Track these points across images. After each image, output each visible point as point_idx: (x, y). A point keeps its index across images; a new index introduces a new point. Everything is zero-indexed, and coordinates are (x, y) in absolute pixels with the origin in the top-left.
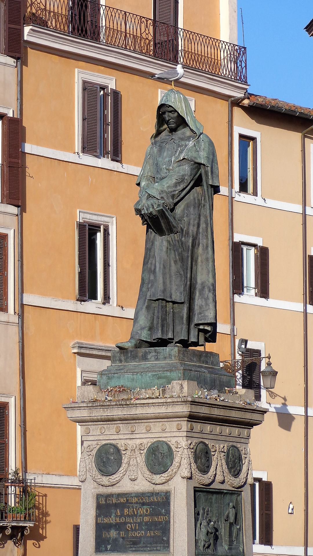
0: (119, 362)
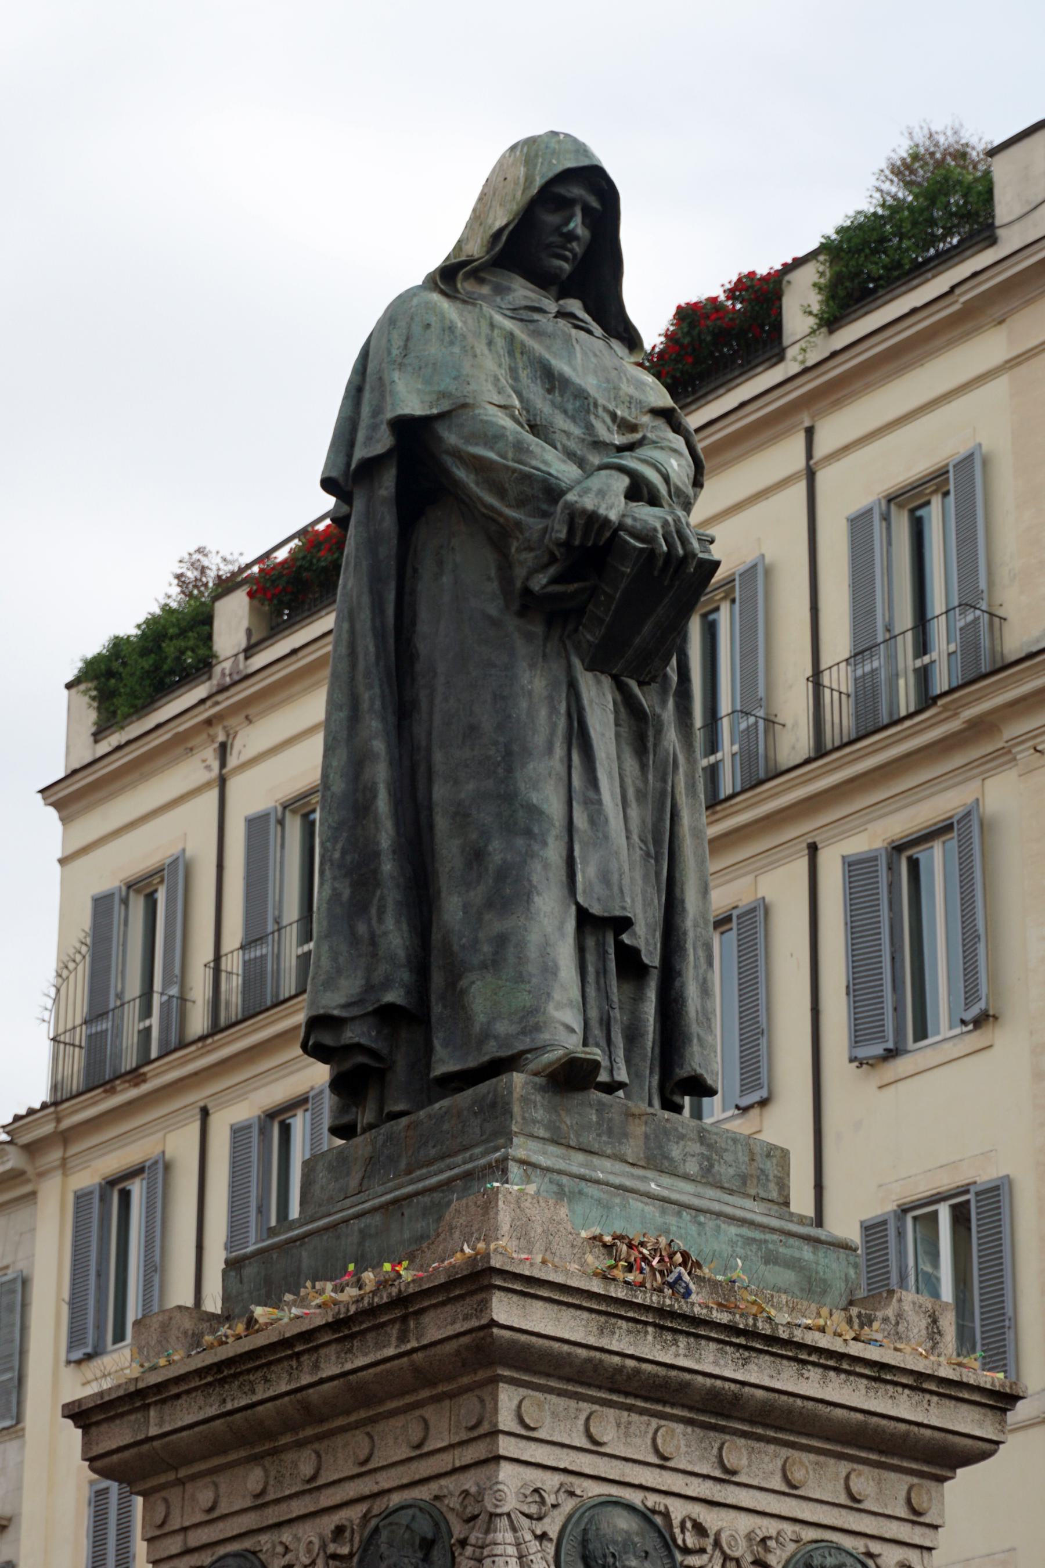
0: (547, 1135)
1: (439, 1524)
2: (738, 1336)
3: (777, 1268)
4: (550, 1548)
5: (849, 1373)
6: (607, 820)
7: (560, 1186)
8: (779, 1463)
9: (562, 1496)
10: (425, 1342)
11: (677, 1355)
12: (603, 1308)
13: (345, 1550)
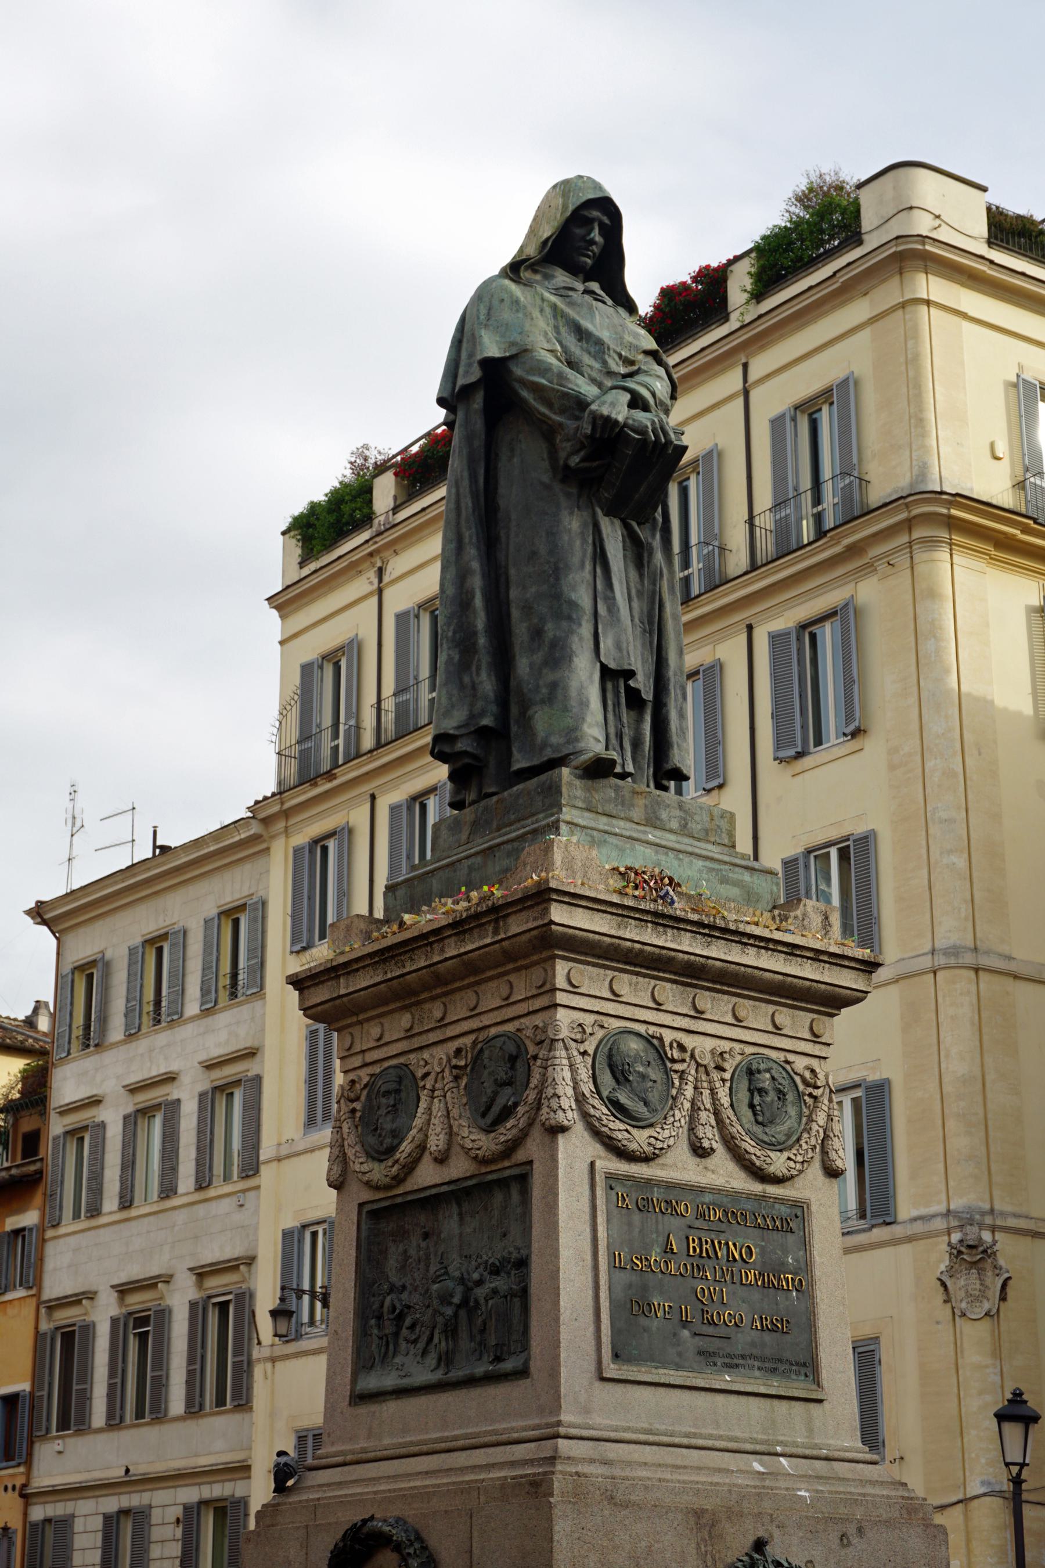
0: (584, 806)
1: (520, 1046)
2: (704, 928)
3: (728, 886)
4: (589, 1060)
5: (773, 950)
6: (619, 610)
7: (592, 837)
8: (731, 1007)
9: (596, 1028)
10: (510, 934)
11: (666, 941)
12: (620, 912)
13: (462, 1063)
